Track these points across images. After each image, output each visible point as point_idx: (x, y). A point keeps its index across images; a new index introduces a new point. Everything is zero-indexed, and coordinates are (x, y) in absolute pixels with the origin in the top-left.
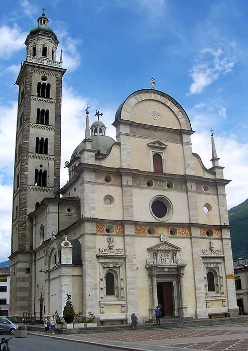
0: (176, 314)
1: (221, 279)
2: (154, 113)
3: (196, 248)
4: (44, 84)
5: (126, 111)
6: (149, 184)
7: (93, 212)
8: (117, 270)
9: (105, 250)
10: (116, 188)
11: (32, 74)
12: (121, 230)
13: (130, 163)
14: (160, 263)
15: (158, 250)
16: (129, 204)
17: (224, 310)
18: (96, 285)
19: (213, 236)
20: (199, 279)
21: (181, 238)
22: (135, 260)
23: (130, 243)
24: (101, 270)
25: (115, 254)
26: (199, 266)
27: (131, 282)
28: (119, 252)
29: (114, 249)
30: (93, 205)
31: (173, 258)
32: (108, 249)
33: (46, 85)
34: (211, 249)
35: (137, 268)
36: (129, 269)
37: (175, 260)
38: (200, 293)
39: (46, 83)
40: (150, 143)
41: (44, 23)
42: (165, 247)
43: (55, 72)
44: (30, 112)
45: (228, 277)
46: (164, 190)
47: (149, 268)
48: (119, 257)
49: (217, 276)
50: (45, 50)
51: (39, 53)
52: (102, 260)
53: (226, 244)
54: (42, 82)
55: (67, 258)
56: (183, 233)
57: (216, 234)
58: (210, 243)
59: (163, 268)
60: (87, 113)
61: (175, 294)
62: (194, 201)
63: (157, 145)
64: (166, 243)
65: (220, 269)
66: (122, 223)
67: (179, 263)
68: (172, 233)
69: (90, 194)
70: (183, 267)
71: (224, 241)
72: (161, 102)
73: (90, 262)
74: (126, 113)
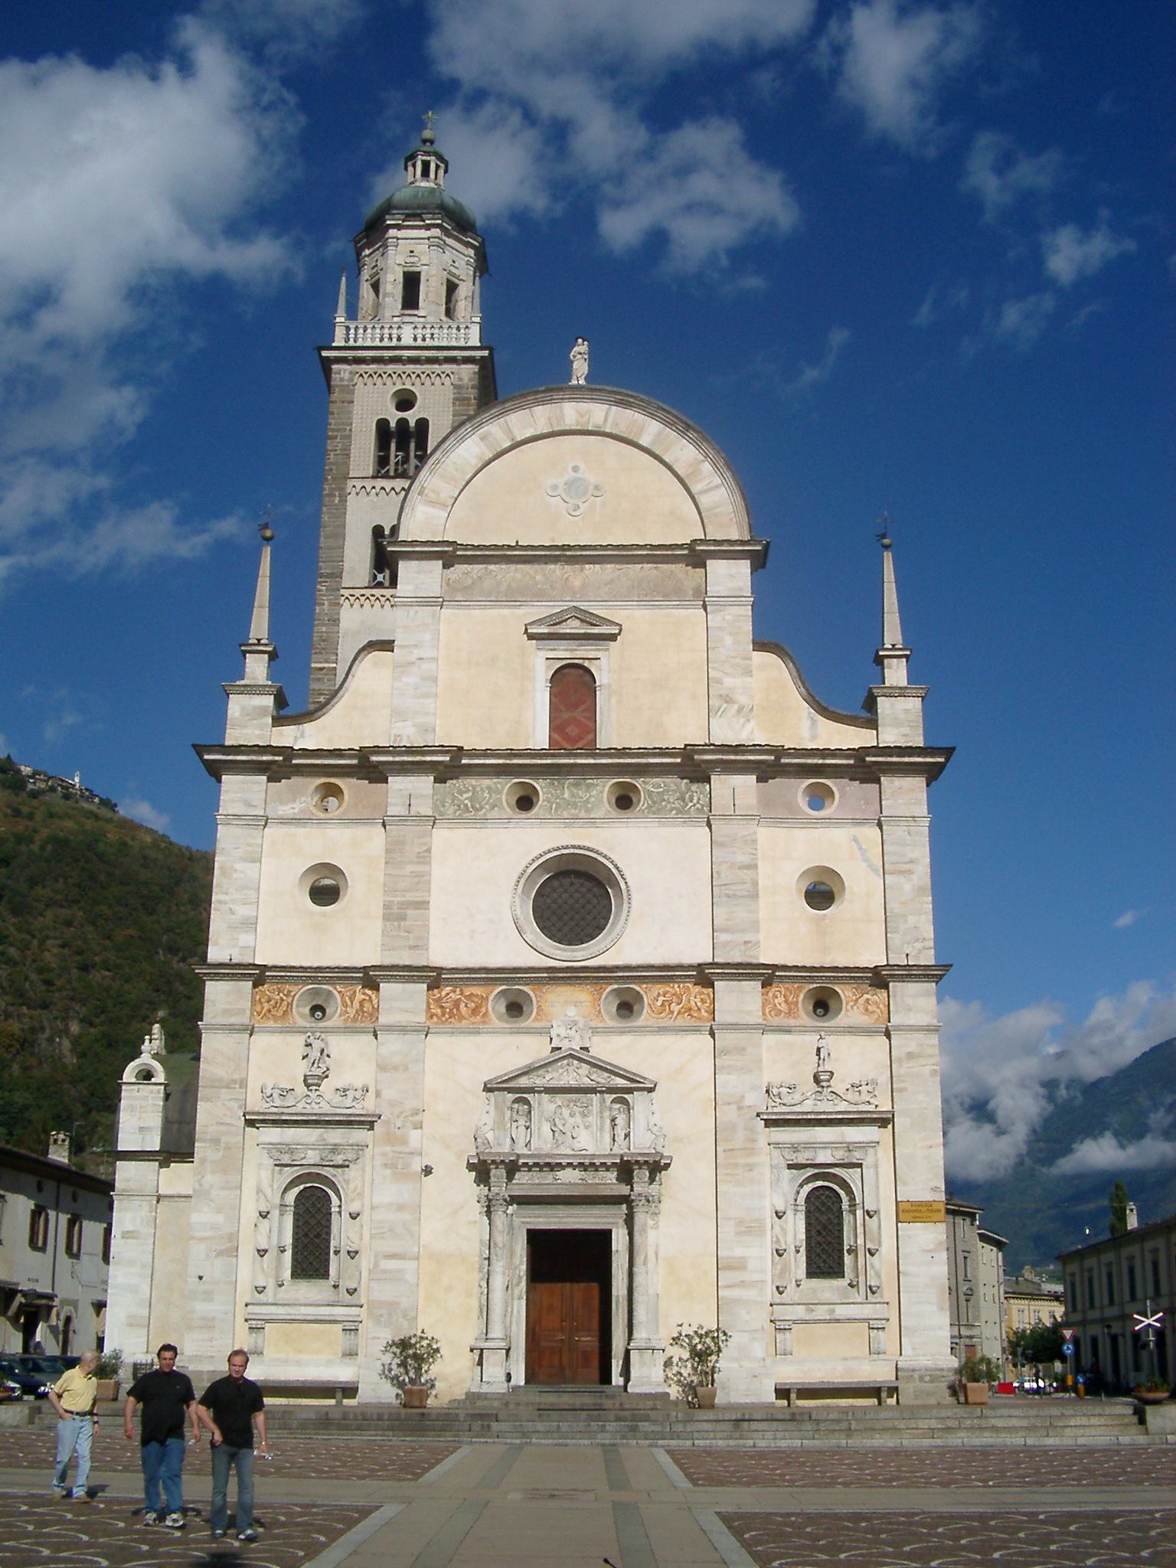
0: (617, 1380)
1: (872, 1223)
2: (575, 487)
3: (733, 1078)
4: (402, 422)
5: (432, 503)
6: (525, 802)
7: (246, 939)
9: (285, 1093)
10: (361, 831)
11: (353, 392)
12: (367, 1006)
14: (542, 1142)
15: (531, 1090)
16: (411, 897)
17: (879, 1372)
18: (234, 1237)
19: (843, 1019)
20: (740, 1222)
21: (662, 1030)
22: (414, 1136)
23: (396, 1060)
24: (265, 1175)
25: (327, 1109)
26: (742, 1161)
27: (391, 1230)
28: (348, 1102)
30: (243, 911)
31: (614, 1126)
32: (301, 1089)
33: (412, 424)
35: (428, 1171)
36: (388, 1172)
37: (620, 1133)
38: (742, 1284)
39: (412, 416)
40: (539, 622)
41: (425, 173)
43: (447, 368)
45: (909, 1212)
46: (592, 822)
47: (481, 1170)
50: (412, 282)
53: (910, 1056)
54: (393, 417)
55: (141, 1129)
56: (675, 1008)
58: (819, 1050)
59: (552, 1167)
62: (742, 858)
63: (573, 627)
66: (369, 978)
67: (641, 1143)
68: (627, 1007)
69: (238, 866)
70: (656, 1167)
73: (216, 1141)
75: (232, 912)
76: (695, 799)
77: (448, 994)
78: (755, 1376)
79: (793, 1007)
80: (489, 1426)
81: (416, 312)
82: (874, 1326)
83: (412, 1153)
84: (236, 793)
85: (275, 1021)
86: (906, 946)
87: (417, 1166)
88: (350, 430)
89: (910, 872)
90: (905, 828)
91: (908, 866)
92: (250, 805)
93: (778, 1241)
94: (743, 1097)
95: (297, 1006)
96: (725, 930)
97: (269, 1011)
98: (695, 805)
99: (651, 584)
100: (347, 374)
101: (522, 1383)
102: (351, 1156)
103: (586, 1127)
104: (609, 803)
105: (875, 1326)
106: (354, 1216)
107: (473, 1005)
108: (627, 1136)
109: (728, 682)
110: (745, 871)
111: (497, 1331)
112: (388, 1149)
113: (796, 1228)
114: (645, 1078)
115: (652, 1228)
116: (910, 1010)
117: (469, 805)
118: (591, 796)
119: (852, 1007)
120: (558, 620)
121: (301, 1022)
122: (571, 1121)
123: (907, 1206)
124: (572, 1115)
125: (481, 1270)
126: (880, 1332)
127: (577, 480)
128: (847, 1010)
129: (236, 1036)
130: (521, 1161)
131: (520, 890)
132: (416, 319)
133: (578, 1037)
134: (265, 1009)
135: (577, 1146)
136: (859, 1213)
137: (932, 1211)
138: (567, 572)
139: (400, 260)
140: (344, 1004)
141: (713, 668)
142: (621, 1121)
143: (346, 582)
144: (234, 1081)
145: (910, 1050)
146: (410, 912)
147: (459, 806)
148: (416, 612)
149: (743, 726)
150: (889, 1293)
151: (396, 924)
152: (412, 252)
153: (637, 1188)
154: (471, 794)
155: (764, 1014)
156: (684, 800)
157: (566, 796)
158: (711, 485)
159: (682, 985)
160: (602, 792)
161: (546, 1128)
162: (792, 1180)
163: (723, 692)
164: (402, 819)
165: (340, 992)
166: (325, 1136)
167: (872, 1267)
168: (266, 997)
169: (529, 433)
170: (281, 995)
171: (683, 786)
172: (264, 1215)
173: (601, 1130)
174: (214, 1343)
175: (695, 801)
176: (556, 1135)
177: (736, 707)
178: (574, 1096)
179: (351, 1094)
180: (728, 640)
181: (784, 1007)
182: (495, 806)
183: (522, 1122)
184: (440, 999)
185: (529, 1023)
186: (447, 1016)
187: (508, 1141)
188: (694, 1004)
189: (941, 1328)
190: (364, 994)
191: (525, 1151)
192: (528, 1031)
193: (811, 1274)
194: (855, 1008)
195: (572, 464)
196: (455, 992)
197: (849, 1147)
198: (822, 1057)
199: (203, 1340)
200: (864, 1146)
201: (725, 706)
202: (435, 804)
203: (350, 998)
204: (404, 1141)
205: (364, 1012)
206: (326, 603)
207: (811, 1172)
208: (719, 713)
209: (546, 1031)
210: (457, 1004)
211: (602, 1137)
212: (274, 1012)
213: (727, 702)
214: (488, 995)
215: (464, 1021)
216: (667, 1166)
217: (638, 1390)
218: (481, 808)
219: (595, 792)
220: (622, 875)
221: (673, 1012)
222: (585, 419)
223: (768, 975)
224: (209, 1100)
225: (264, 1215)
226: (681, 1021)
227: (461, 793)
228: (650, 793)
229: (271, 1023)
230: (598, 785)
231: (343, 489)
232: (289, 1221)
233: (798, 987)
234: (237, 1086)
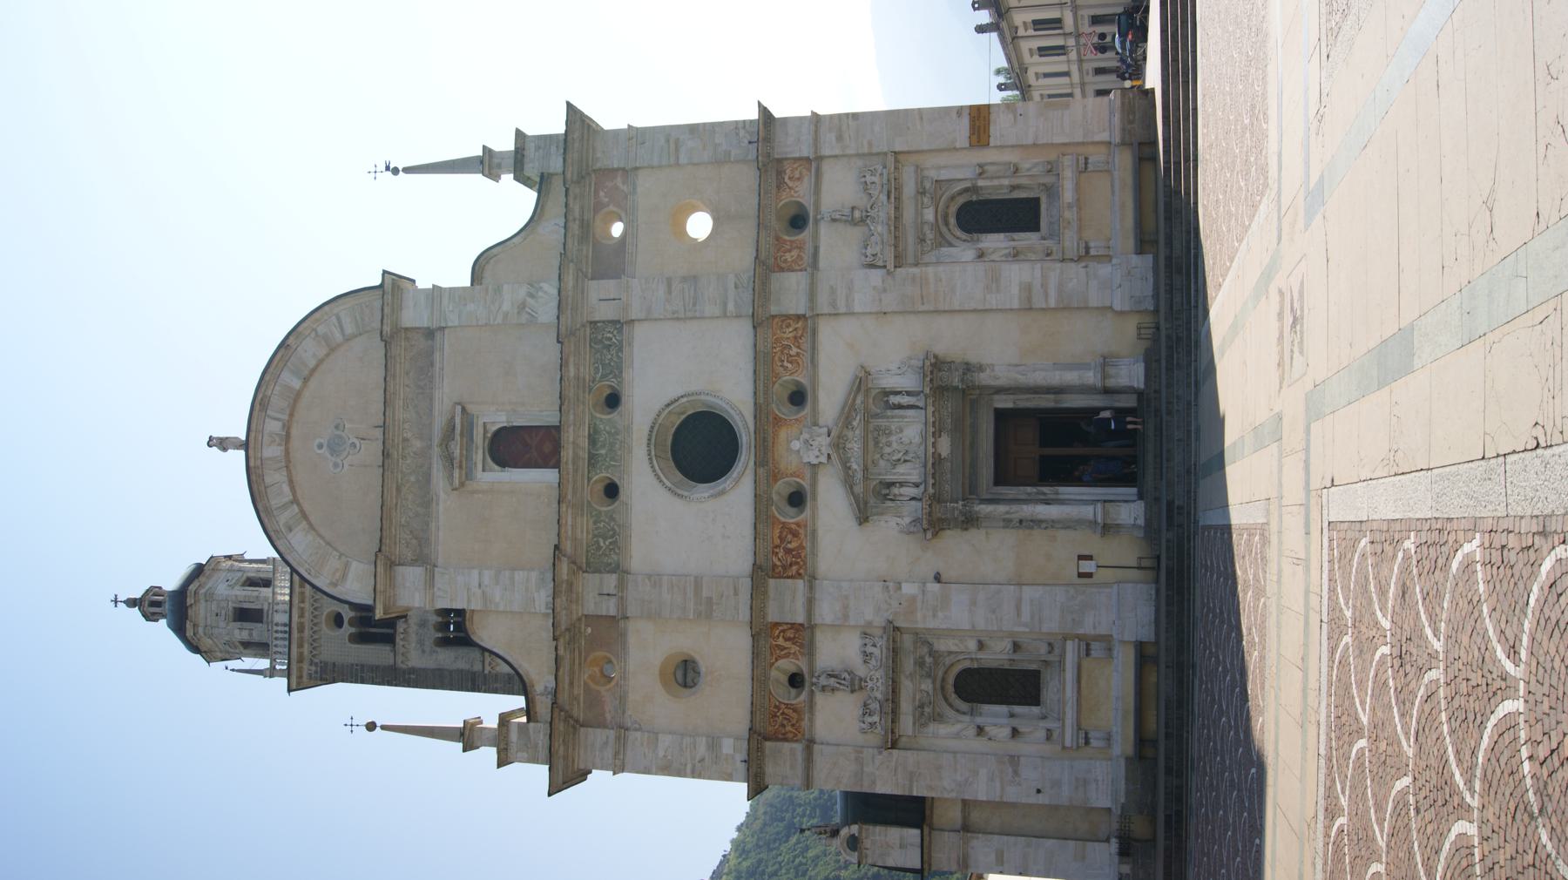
0: (1129, 402)
5: (344, 576)
6: (612, 491)
7: (727, 746)
8: (948, 661)
9: (867, 711)
11: (326, 664)
12: (790, 634)
13: (534, 575)
19: (807, 201)
21: (814, 362)
24: (943, 729)
27: (994, 612)
29: (861, 671)
30: (702, 749)
31: (900, 407)
34: (856, 218)
36: (940, 614)
37: (905, 400)
38: (1044, 286)
40: (451, 477)
42: (855, 447)
44: (451, 672)
46: (628, 429)
48: (895, 652)
49: (974, 189)
51: (256, 632)
52: (906, 724)
53: (840, 138)
54: (348, 630)
55: (901, 846)
56: (794, 351)
57: (801, 192)
58: (834, 220)
59: (938, 460)
60: (371, 727)
61: (1046, 402)
64: (839, 445)
65: (945, 175)
71: (826, 151)
72: (291, 415)
74: (351, 576)
75: (702, 760)
76: (609, 335)
77: (779, 559)
78: (1129, 273)
79: (794, 245)
80: (1178, 508)
81: (265, 611)
82: (1084, 167)
83: (923, 591)
84: (595, 756)
85: (803, 720)
86: (743, 145)
87: (934, 587)
88: (357, 665)
89: (677, 141)
90: (638, 147)
91: (672, 146)
92: (606, 743)
93: (1006, 255)
94: (874, 288)
95: (789, 700)
96: (725, 304)
97: (793, 725)
98: (615, 336)
99: (422, 377)
100: (311, 668)
101: (1134, 490)
102: (925, 650)
103: (901, 431)
104: (609, 413)
105: (1083, 166)
106: (981, 646)
107: (790, 537)
108: (909, 393)
109: (506, 307)
110: (673, 287)
111: (1087, 512)
112: (919, 615)
113: (995, 242)
114: (857, 377)
115: (993, 370)
116: (799, 140)
117: (610, 540)
118: (605, 430)
119: (796, 192)
120: (449, 459)
121: (804, 696)
122: (895, 445)
123: (975, 138)
124: (889, 445)
125: (1032, 528)
126: (1090, 161)
127: (328, 446)
128: (799, 196)
129: (817, 757)
130: (931, 491)
131: (686, 494)
132: (270, 612)
133: (819, 439)
134: (791, 729)
135: (917, 440)
136: (981, 183)
137: (979, 117)
138: (409, 453)
139: (222, 624)
140: (787, 656)
141: (495, 320)
142: (894, 399)
143: (477, 667)
144: (856, 759)
145: (834, 139)
146: (705, 593)
147: (611, 550)
148: (439, 589)
149: (546, 292)
150: (1053, 156)
151: (714, 607)
152: (217, 615)
153: (956, 382)
154: (601, 541)
155: (801, 270)
156: (610, 345)
157: (603, 452)
158: (337, 324)
159: (775, 345)
160: (601, 420)
161: (901, 469)
162: (951, 245)
163: (516, 311)
164: (622, 602)
165: (777, 660)
166: (908, 673)
167: (1028, 170)
168: (781, 729)
169: (286, 488)
170: (778, 714)
171: (596, 346)
172: (980, 730)
173: (902, 417)
174: (1100, 778)
175: (611, 335)
176: (907, 458)
177: (529, 300)
178: (871, 443)
179: (870, 649)
180: (471, 307)
181: (795, 253)
182: (611, 516)
183: (896, 490)
184: (784, 567)
185: (806, 484)
186: (799, 560)
187: (913, 502)
188: (791, 335)
189: (1085, 106)
190: (778, 637)
191: (922, 487)
192: (814, 484)
193: (1036, 228)
194: (797, 189)
195: (316, 448)
196: (777, 553)
197: (922, 192)
198: (838, 217)
199: (1097, 789)
200: (920, 181)
201: (527, 309)
202: (608, 572)
203: (782, 650)
204: (913, 599)
205: (794, 638)
206: (495, 685)
207: (944, 229)
208: (534, 314)
209: (814, 467)
210: (788, 551)
211: (910, 417)
212: (794, 722)
213: (524, 308)
214: (780, 522)
215: (804, 544)
216: (936, 357)
217: (1142, 379)
218: (613, 529)
219: (601, 426)
220: (676, 401)
221: (797, 353)
222: (277, 439)
223: (767, 267)
224: (874, 782)
225: (980, 730)
226: (806, 345)
227: (599, 548)
228: (603, 376)
229: (805, 723)
230: (595, 424)
231: (404, 672)
232: (987, 708)
233: (777, 240)
234: (861, 755)
